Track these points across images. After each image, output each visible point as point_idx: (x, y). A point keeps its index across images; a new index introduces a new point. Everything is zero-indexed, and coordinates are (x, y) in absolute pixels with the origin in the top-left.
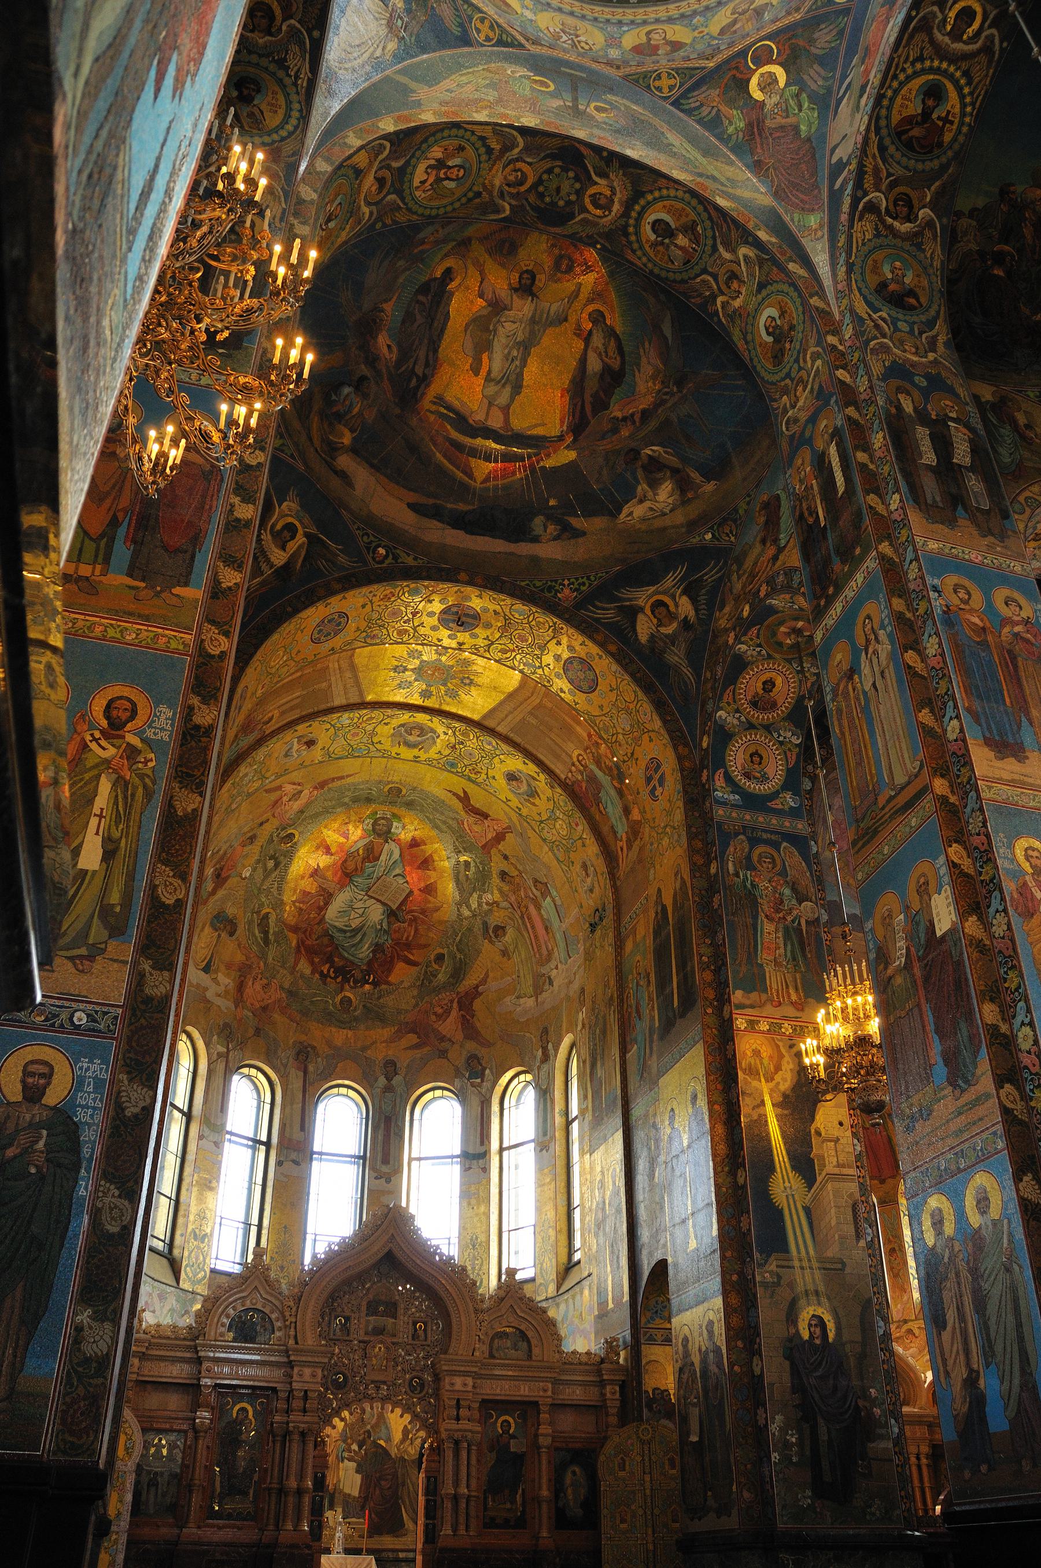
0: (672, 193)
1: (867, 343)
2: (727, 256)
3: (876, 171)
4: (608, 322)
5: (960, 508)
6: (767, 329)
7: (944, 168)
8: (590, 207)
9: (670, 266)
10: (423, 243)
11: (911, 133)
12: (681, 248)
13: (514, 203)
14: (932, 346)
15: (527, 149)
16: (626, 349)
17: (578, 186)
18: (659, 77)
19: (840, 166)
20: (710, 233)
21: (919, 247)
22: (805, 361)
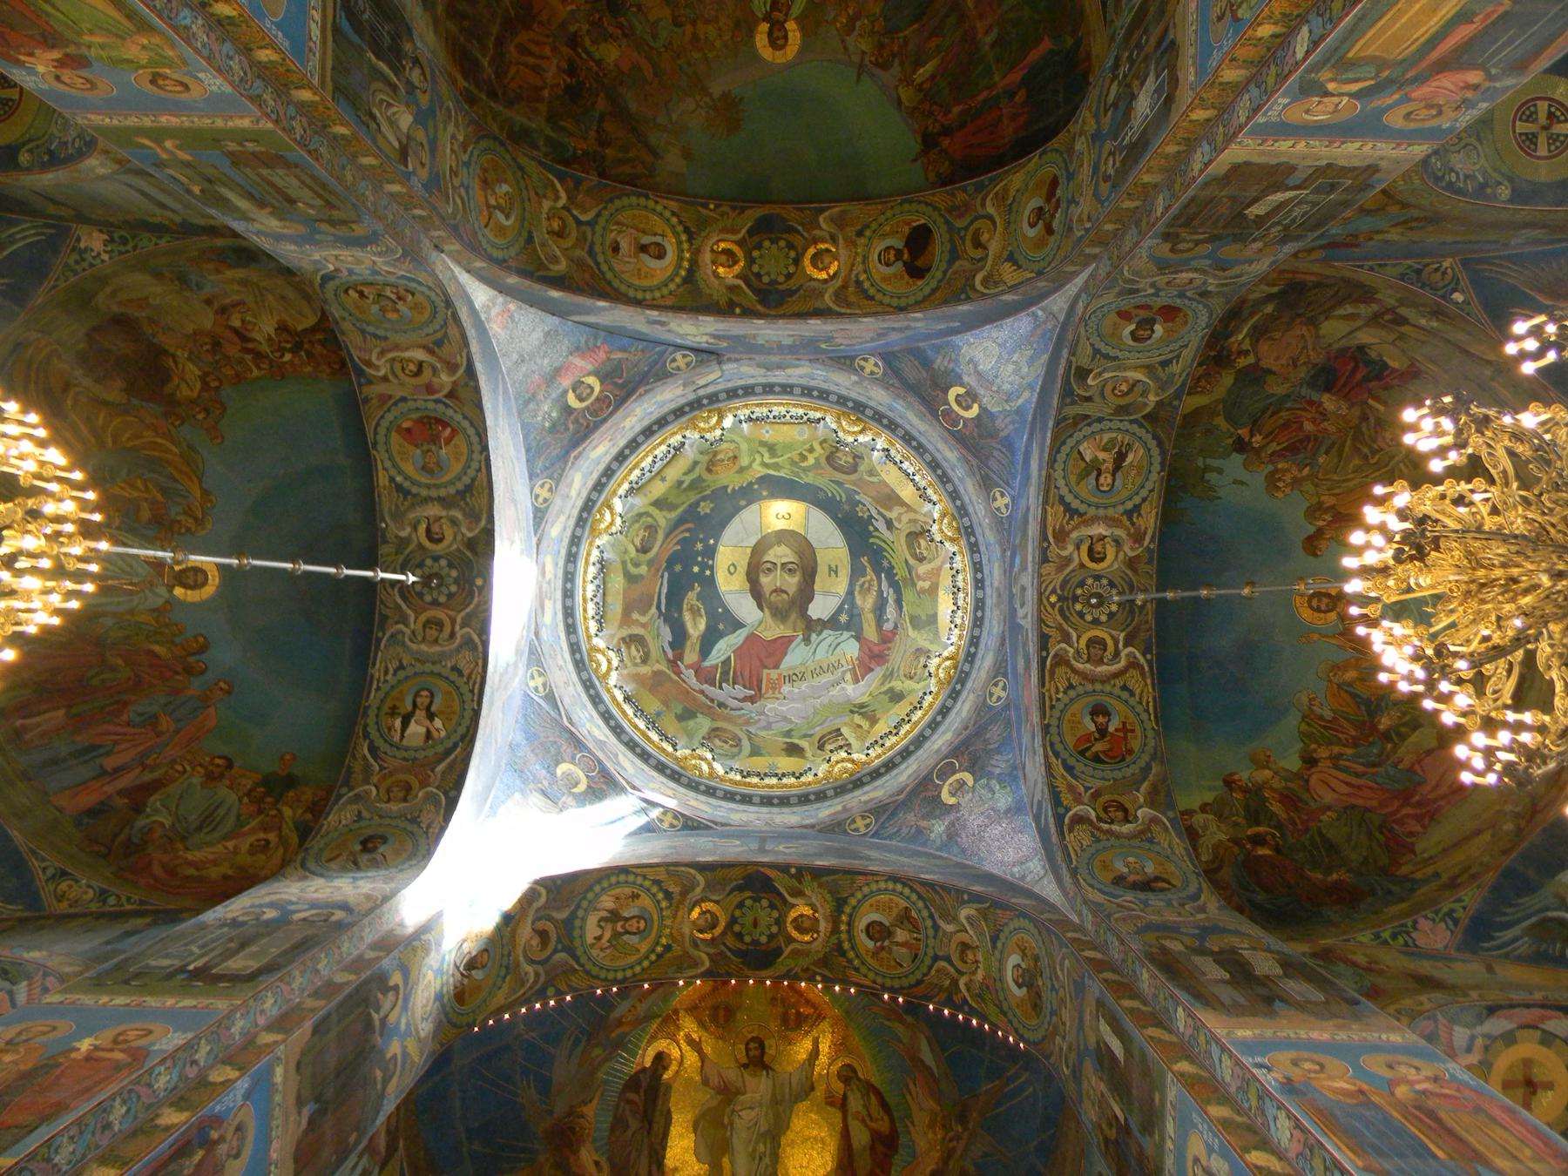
0: (874, 887)
1: (1109, 916)
2: (950, 928)
3: (1071, 789)
4: (860, 1074)
5: (1277, 1004)
6: (1016, 983)
7: (1147, 769)
8: (795, 934)
9: (901, 970)
10: (619, 1023)
11: (1094, 749)
12: (903, 944)
13: (712, 951)
14: (1202, 909)
15: (710, 886)
16: (892, 1101)
17: (775, 914)
18: (854, 821)
19: (1040, 803)
20: (925, 913)
21: (1151, 841)
22: (1057, 978)
